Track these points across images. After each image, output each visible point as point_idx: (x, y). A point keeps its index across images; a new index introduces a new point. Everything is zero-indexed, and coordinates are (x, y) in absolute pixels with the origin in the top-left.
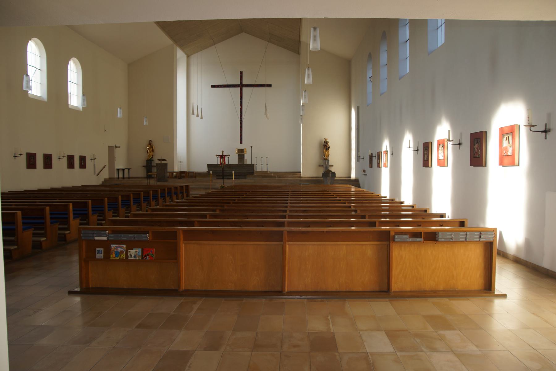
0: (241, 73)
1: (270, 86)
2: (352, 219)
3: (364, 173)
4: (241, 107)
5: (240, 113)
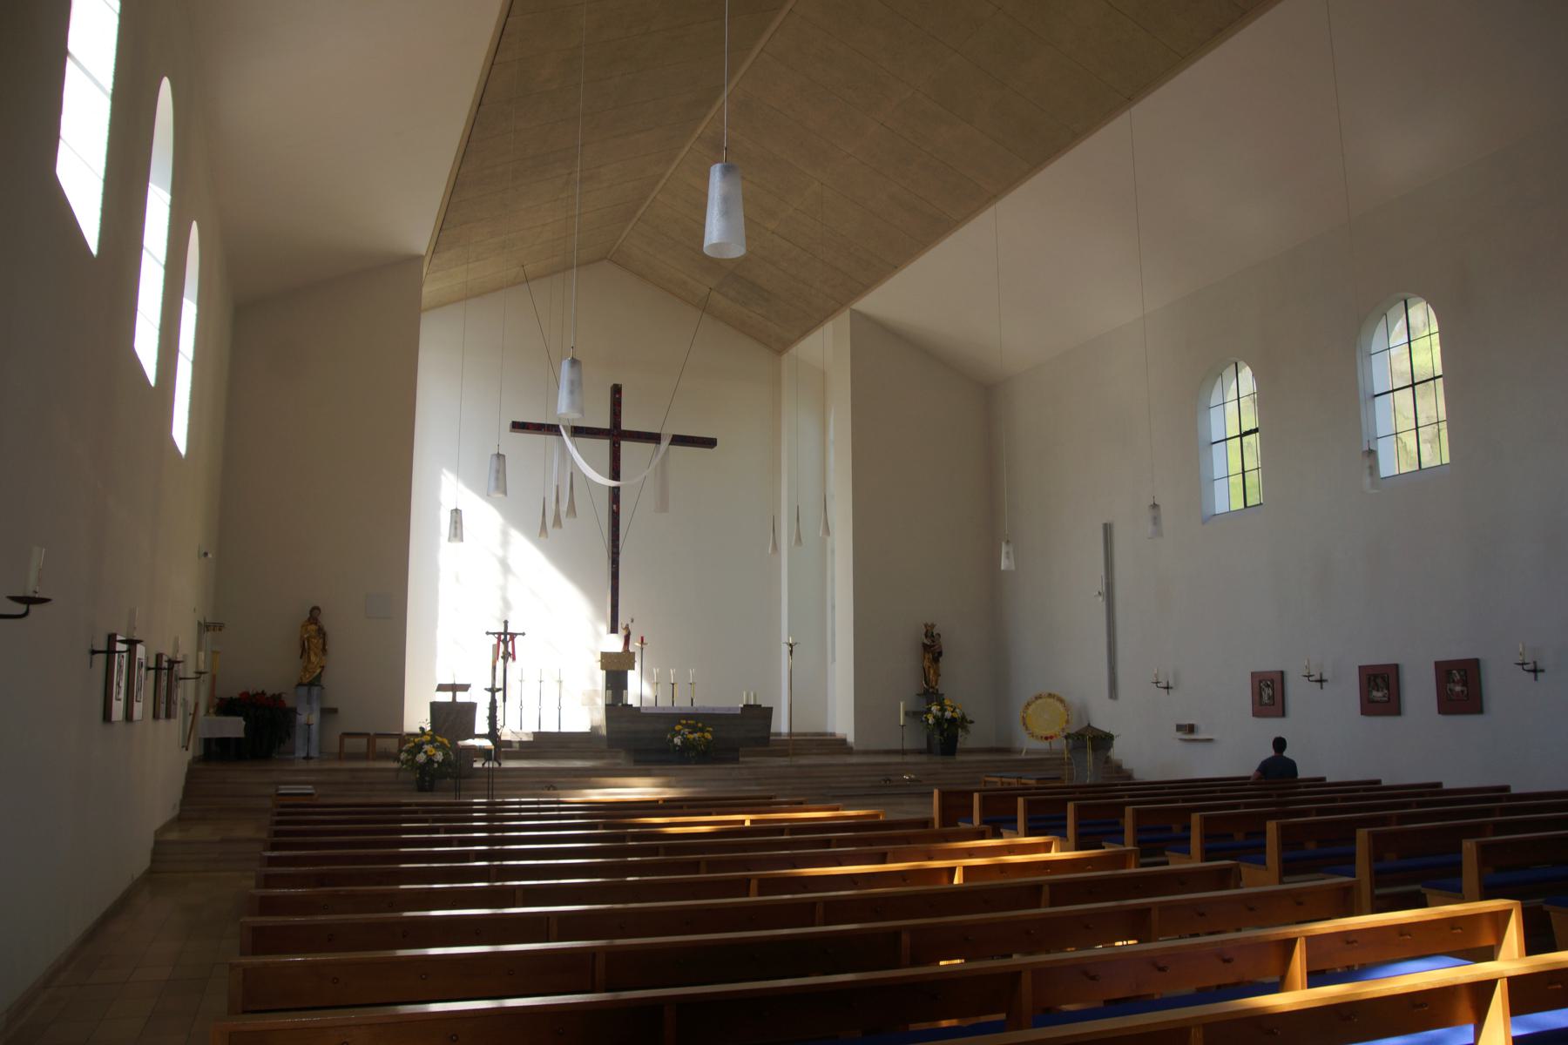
0: (616, 391)
1: (710, 443)
2: (629, 879)
3: (1180, 735)
4: (615, 506)
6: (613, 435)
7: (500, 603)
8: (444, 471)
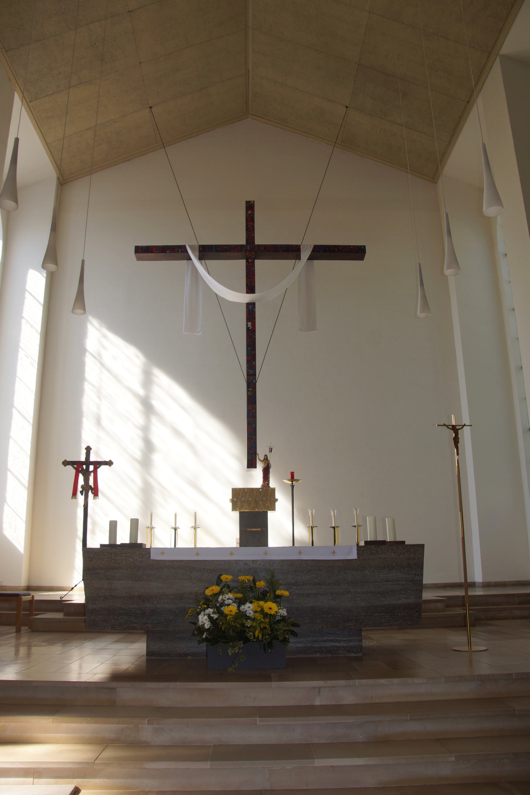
0: (250, 207)
4: (250, 324)
5: (248, 345)
6: (245, 251)
7: (140, 443)
8: (90, 318)
